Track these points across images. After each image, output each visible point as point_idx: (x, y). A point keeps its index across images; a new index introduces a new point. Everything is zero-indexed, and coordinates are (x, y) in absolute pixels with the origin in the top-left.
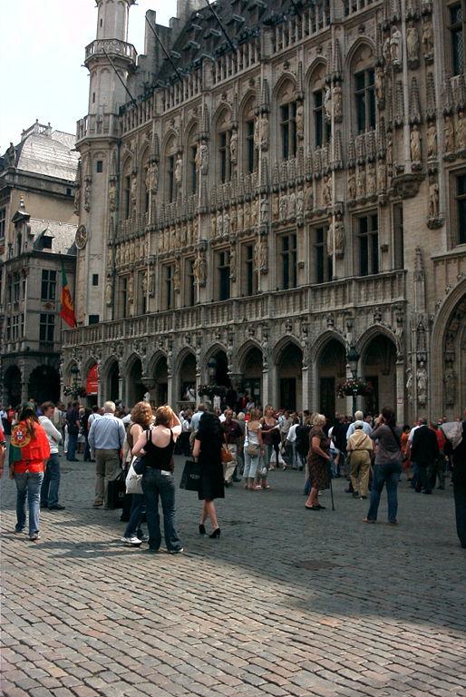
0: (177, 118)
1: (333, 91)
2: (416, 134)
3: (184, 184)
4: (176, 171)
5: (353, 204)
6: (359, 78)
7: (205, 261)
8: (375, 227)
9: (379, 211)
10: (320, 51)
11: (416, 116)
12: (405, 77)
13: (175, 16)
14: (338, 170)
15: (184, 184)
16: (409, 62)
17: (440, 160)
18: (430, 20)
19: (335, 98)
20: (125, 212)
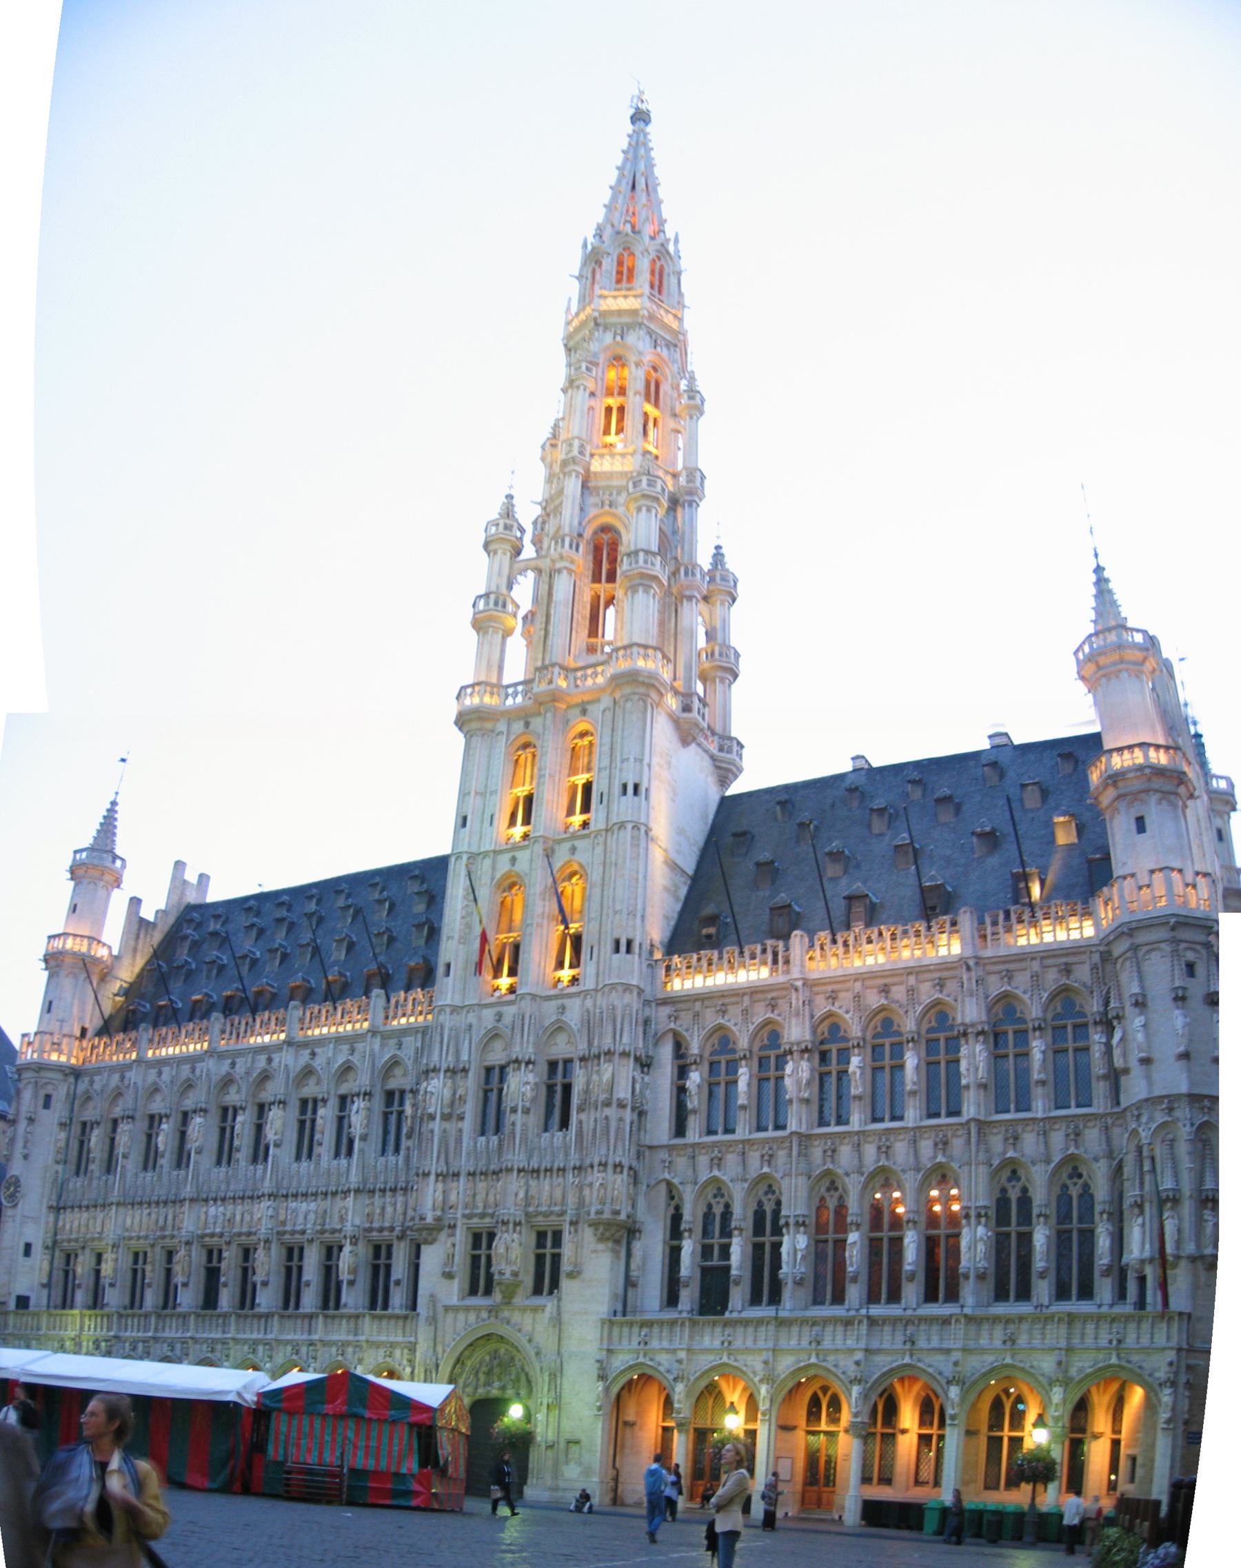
0: (166, 1070)
1: (362, 1105)
2: (440, 1186)
3: (167, 1155)
4: (160, 1138)
5: (370, 1230)
6: (390, 1095)
7: (190, 1256)
8: (389, 1256)
9: (395, 1243)
10: (352, 1051)
11: (442, 1168)
12: (436, 1125)
13: (163, 908)
14: (357, 1191)
15: (167, 1155)
16: (442, 1114)
17: (459, 1215)
18: (466, 1077)
19: (363, 1113)
20: (73, 1168)
